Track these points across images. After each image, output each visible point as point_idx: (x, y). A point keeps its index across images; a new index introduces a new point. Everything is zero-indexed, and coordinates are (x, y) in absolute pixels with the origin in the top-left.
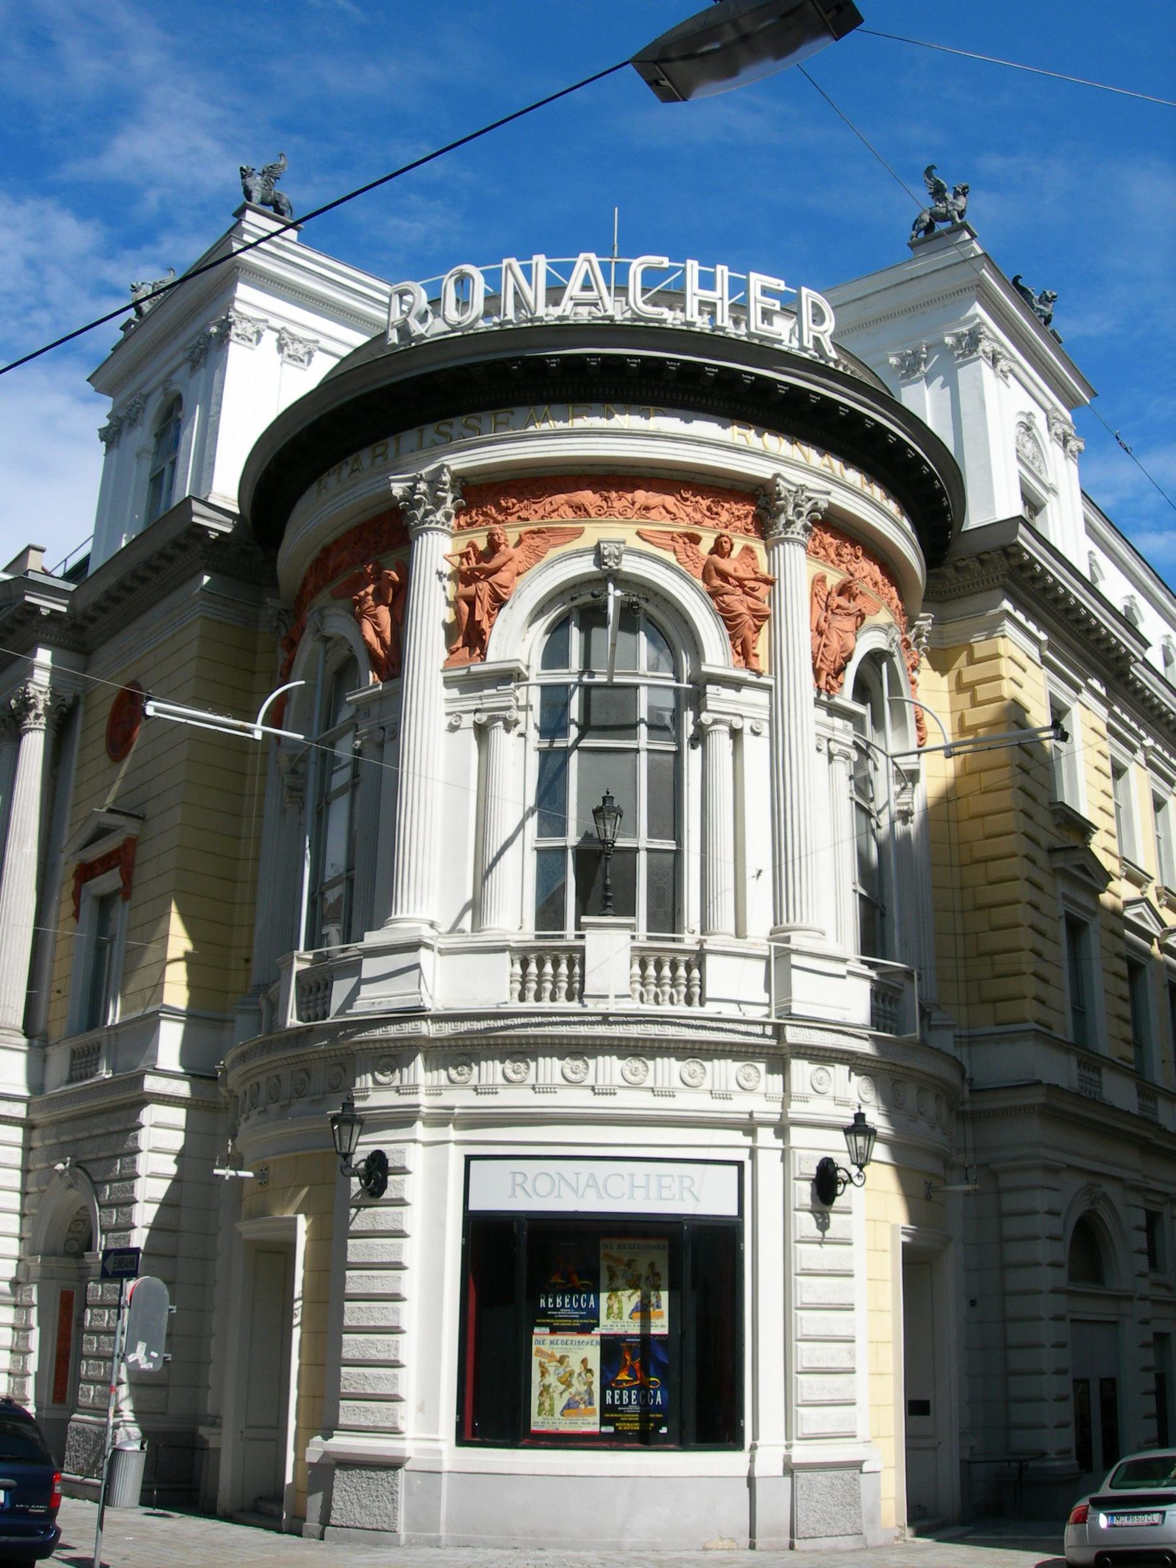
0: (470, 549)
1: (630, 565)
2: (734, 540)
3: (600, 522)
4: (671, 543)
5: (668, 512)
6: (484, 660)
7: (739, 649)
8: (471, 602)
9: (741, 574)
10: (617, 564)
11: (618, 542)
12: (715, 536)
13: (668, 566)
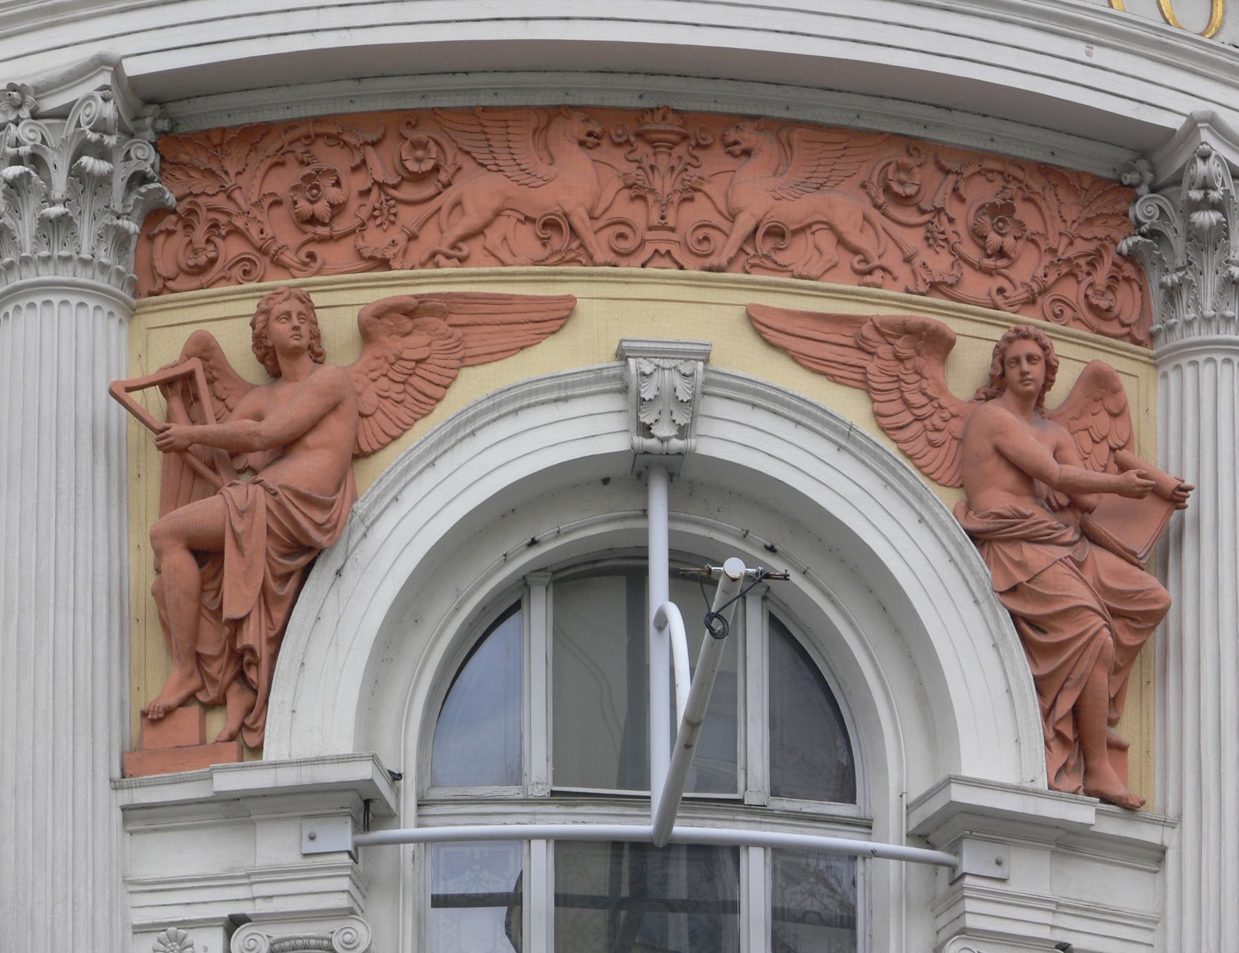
0: (196, 365)
1: (731, 437)
2: (1059, 348)
3: (626, 280)
4: (854, 357)
5: (841, 242)
6: (258, 750)
7: (1068, 732)
8: (208, 553)
9: (1075, 470)
10: (683, 432)
11: (688, 356)
12: (998, 334)
13: (844, 437)
